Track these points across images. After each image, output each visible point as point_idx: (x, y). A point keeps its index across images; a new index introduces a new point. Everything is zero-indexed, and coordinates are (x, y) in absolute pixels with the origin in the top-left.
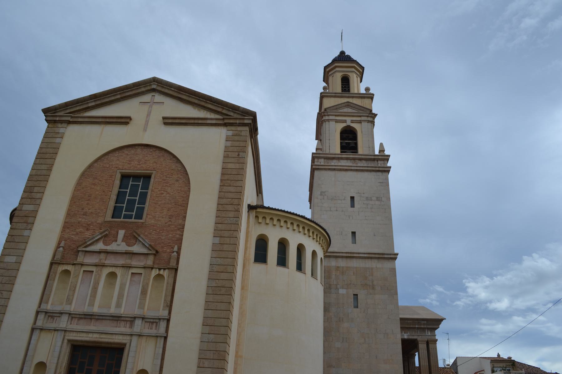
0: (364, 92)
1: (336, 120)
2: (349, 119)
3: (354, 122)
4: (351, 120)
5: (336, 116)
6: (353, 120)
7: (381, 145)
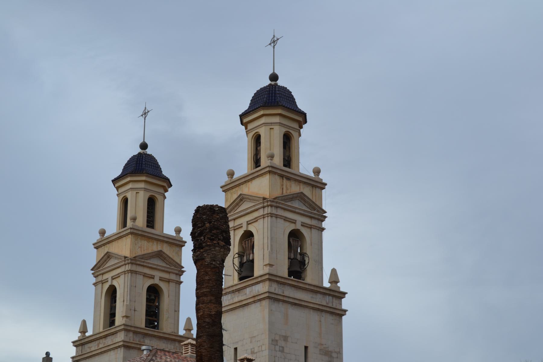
0: (312, 175)
1: (286, 217)
2: (300, 219)
3: (304, 225)
4: (302, 222)
5: (285, 209)
6: (304, 223)
7: (334, 272)
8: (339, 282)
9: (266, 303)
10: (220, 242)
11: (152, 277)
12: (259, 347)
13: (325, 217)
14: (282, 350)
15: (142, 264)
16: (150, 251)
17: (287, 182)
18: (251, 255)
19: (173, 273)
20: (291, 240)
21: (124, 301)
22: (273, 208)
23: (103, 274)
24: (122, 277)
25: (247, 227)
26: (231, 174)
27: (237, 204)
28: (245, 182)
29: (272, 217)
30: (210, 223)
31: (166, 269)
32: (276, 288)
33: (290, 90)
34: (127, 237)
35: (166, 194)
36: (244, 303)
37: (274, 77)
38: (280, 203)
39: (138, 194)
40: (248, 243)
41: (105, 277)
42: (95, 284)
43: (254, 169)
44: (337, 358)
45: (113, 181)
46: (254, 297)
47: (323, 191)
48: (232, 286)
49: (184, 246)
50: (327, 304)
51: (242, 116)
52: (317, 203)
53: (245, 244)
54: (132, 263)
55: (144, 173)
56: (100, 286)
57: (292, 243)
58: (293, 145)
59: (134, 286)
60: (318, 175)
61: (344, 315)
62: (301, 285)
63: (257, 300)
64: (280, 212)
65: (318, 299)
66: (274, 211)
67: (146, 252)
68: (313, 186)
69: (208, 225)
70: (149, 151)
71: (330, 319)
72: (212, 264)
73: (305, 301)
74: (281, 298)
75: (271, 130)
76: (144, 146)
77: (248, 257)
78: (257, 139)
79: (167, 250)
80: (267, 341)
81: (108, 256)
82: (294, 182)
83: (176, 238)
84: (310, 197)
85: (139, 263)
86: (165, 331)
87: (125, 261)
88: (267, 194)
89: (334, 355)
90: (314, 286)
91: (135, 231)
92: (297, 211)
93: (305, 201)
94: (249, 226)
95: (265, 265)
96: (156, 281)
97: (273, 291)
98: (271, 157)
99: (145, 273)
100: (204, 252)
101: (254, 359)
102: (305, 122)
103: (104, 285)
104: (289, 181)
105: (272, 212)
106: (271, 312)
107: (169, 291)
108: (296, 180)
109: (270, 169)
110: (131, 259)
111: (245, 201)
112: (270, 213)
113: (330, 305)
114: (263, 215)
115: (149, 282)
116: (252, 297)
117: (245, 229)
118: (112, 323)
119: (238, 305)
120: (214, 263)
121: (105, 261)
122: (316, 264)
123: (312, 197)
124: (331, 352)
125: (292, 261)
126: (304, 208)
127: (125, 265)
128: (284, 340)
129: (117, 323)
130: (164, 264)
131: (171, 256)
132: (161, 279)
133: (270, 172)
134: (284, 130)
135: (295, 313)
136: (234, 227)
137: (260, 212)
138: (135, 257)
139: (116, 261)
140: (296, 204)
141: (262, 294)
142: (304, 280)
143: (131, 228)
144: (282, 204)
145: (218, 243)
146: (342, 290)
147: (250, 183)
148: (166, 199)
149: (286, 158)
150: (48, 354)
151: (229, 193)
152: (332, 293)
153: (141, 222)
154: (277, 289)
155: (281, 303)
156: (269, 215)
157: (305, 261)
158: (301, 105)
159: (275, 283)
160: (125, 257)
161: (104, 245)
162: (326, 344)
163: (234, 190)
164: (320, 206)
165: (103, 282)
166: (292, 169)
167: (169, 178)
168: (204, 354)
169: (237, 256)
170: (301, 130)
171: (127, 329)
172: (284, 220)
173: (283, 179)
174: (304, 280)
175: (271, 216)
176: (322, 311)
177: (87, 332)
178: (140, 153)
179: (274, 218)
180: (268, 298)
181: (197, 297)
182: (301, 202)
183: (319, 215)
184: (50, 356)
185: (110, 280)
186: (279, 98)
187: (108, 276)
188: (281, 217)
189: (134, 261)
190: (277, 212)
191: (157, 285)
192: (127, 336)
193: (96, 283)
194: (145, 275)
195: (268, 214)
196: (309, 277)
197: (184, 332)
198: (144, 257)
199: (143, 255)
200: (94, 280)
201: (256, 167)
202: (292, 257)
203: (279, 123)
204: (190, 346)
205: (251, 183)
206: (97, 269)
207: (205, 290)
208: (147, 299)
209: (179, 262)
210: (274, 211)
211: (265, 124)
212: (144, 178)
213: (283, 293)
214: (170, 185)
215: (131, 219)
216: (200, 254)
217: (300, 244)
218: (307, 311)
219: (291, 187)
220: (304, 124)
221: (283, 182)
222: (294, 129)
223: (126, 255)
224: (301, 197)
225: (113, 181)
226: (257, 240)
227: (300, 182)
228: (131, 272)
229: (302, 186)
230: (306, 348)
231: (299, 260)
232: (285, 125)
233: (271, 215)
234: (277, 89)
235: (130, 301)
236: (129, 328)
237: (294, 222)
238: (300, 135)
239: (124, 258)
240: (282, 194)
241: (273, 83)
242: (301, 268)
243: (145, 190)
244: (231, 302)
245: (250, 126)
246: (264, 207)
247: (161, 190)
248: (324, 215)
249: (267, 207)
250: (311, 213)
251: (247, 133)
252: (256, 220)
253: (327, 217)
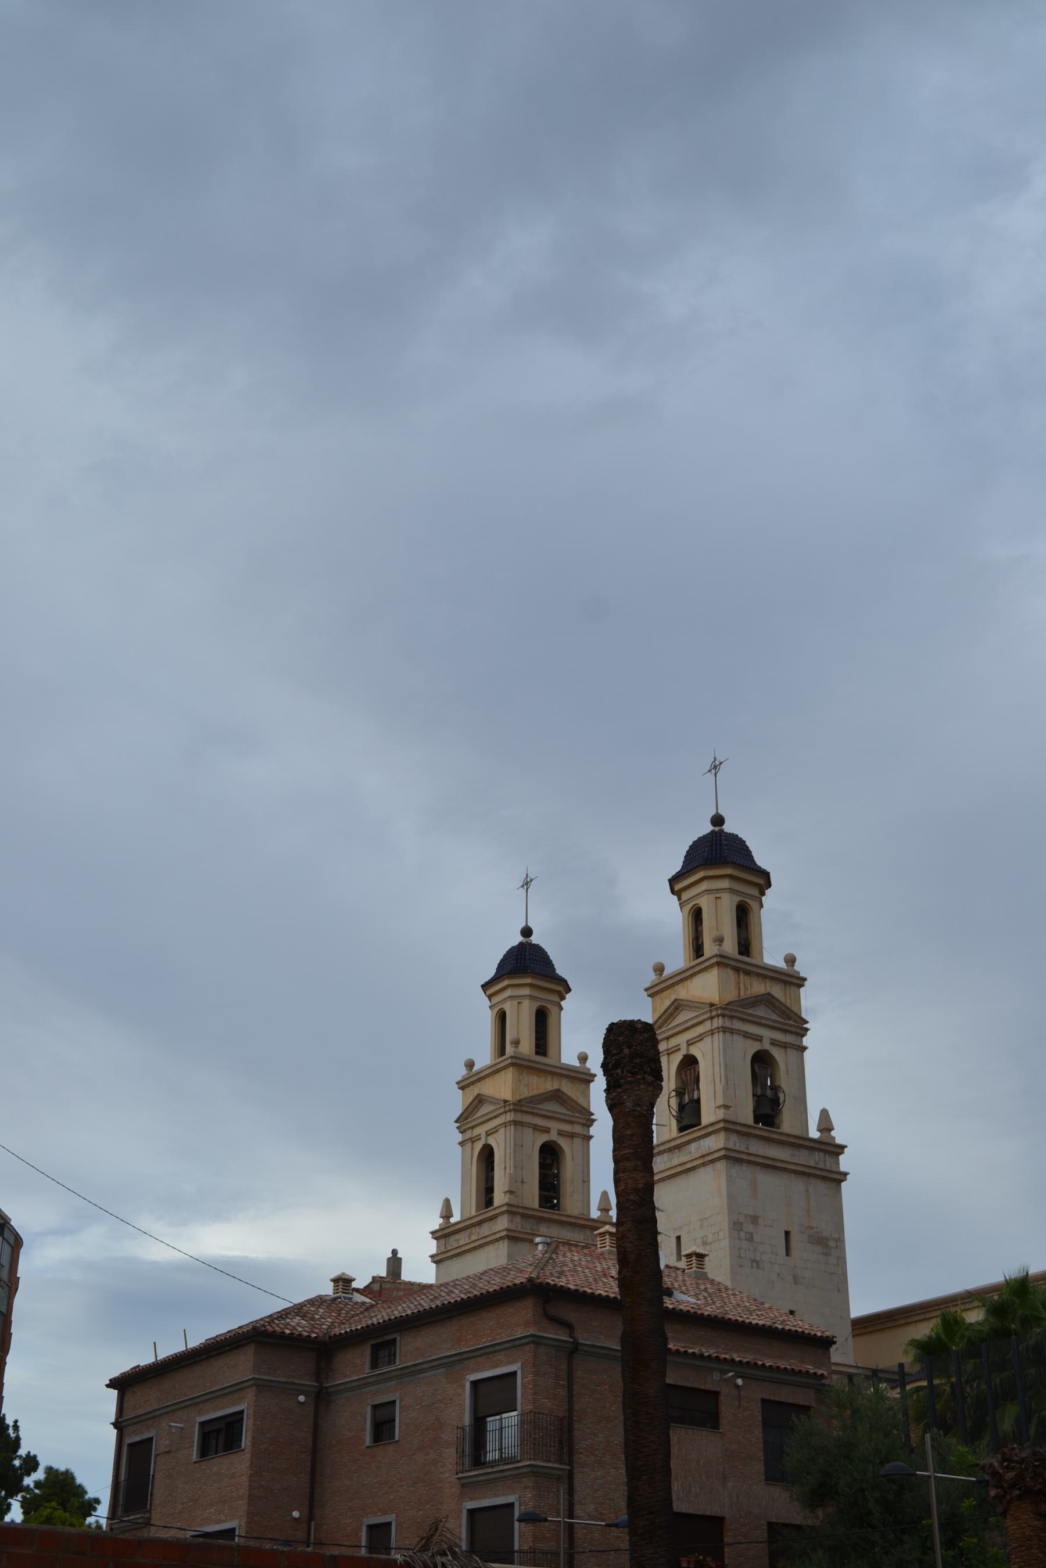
2: (767, 1034)
4: (771, 1039)
5: (743, 1020)
6: (774, 1040)
7: (824, 1114)
8: (833, 1129)
9: (721, 1166)
10: (646, 1076)
11: (547, 1131)
12: (714, 1234)
13: (807, 1030)
14: (750, 1238)
15: (531, 1110)
16: (542, 1091)
17: (746, 978)
18: (696, 1092)
19: (579, 1123)
20: (756, 1068)
21: (505, 1168)
22: (726, 1018)
23: (472, 1128)
24: (502, 1131)
25: (688, 1049)
26: (659, 969)
27: (671, 1015)
28: (682, 980)
29: (724, 1032)
30: (630, 1047)
31: (567, 1118)
32: (735, 1143)
33: (744, 839)
34: (507, 1070)
35: (563, 1003)
36: (689, 1166)
37: (718, 820)
38: (736, 1011)
39: (520, 1005)
40: (690, 1075)
41: (477, 1131)
42: (461, 1144)
43: (693, 960)
44: (837, 1247)
45: (483, 986)
46: (703, 1156)
47: (802, 989)
48: (669, 1141)
49: (593, 1081)
50: (817, 1164)
51: (672, 881)
52: (793, 1009)
53: (686, 1076)
54: (515, 1110)
55: (528, 973)
56: (469, 1145)
57: (757, 1071)
58: (752, 921)
59: (520, 1144)
60: (793, 966)
61: (843, 1181)
62: (775, 1136)
63: (708, 1161)
64: (737, 1025)
65: (802, 1158)
66: (728, 1024)
67: (536, 1092)
68: (786, 983)
69: (626, 1051)
70: (534, 939)
71: (822, 1187)
72: (635, 1110)
74: (745, 1157)
75: (718, 900)
76: (527, 932)
77: (691, 1095)
78: (697, 915)
79: (568, 1088)
80: (726, 1225)
81: (480, 1100)
83: (581, 1070)
84: (783, 1000)
85: (525, 1109)
86: (569, 1212)
87: (505, 1107)
88: (715, 998)
89: (832, 1244)
90: (795, 1137)
91: (519, 1062)
92: (763, 1021)
94: (691, 1047)
95: (719, 1107)
96: (553, 1136)
97: (731, 1145)
98: (720, 940)
99: (536, 1125)
100: (622, 1092)
101: (707, 1253)
102: (769, 885)
103: (475, 1144)
104: (748, 977)
105: (725, 1026)
106: (730, 1179)
107: (572, 1151)
108: (759, 975)
109: (719, 959)
110: (514, 1104)
111: (682, 1010)
112: (722, 1027)
113: (821, 1166)
114: (712, 1030)
115: (543, 1138)
116: (699, 1158)
117: (685, 1053)
118: (489, 1202)
119: (679, 1169)
120: (638, 1109)
121: (476, 1107)
123: (786, 1002)
124: (827, 1239)
125: (759, 1100)
126: (774, 1017)
127: (506, 1112)
128: (753, 1223)
129: (497, 1202)
130: (564, 1111)
131: (574, 1098)
132: (561, 1133)
133: (718, 964)
134: (737, 899)
135: (767, 1181)
136: (668, 1050)
137: (707, 1026)
138: (519, 1101)
139: (492, 1108)
140: (761, 1011)
141: (715, 1152)
142: (779, 1128)
143: (512, 1057)
144: (740, 1012)
145: (644, 1079)
146: (838, 1141)
147: (689, 982)
148: (562, 1011)
149: (743, 942)
150: (394, 1252)
151: (657, 998)
152: (822, 1147)
153: (527, 1047)
154: (738, 1144)
155: (745, 1165)
156: (721, 1029)
157: (779, 1098)
158: (761, 860)
159: (735, 1134)
160: (505, 1101)
161: (473, 1083)
162: (817, 1228)
163: (665, 993)
164: (798, 1013)
165: (473, 1140)
166: (752, 958)
167: (566, 979)
168: (629, 1250)
169: (674, 1094)
170: (763, 898)
171: (512, 1210)
172: (744, 1036)
173: (739, 974)
174: (779, 1128)
175: (723, 1031)
176: (809, 1175)
177: (452, 1216)
178: (521, 944)
179: (728, 1035)
180: (725, 1157)
181: (614, 1161)
183: (797, 1027)
184: (398, 1256)
185: (483, 1136)
186: (726, 851)
187: (481, 1130)
188: (739, 1032)
189: (519, 1106)
190: (732, 1024)
191: (554, 1142)
192: (512, 1221)
193: (463, 1142)
194: (536, 1128)
195: (718, 1028)
196: (787, 1124)
197: (599, 1213)
198: (534, 1100)
199: (533, 1097)
200: (459, 1137)
201: (698, 957)
202: (759, 1092)
203: (730, 889)
204: (607, 1236)
205: (691, 981)
206: (464, 1121)
207: (626, 1151)
208: (540, 1164)
209: (586, 1107)
210: (728, 1024)
211: (708, 891)
212: (528, 981)
213: (748, 1149)
214: (568, 990)
215: (512, 1043)
216: (616, 1096)
217: (769, 1072)
219: (751, 985)
220: (767, 889)
221: (739, 978)
222: (752, 897)
223: (507, 1099)
224: (767, 1000)
225: (483, 986)
226: (704, 1068)
227: (765, 977)
228: (516, 1123)
229: (768, 983)
230: (787, 1234)
231: (770, 1096)
232: (737, 891)
233: (724, 1030)
234: (723, 838)
235: (515, 1167)
236: (515, 1210)
237: (759, 1039)
238: (761, 906)
239: (502, 1102)
240: (739, 996)
241: (717, 829)
242: (773, 1111)
243: (532, 998)
244: (669, 1166)
245: (685, 896)
246: (712, 1018)
247: (556, 998)
248: (805, 1026)
249: (717, 1018)
250: (785, 1024)
251: (681, 905)
252: (701, 1038)
253: (809, 1029)
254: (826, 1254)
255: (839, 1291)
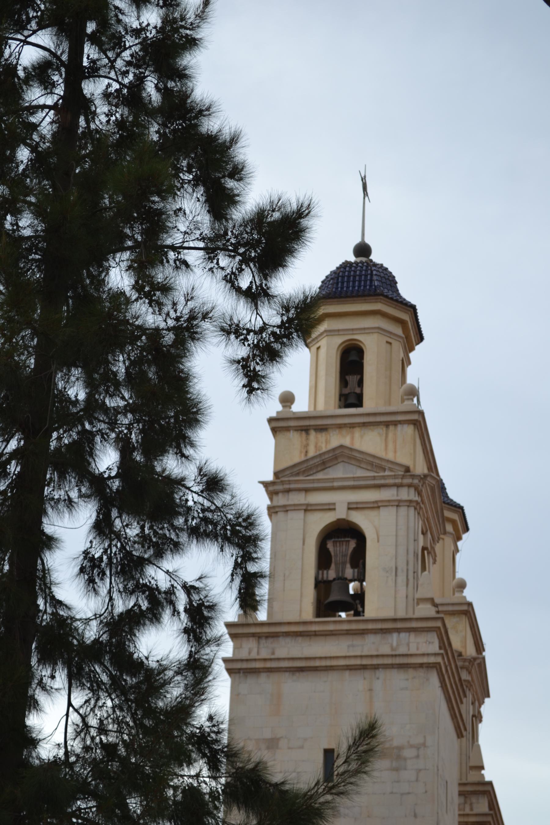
20: (330, 546)
38: (290, 482)
44: (418, 757)
62: (331, 627)
73: (321, 658)
82: (337, 431)
92: (336, 484)
93: (355, 459)
122: (387, 577)
124: (400, 748)
134: (339, 340)
172: (306, 510)
176: (376, 667)
182: (351, 464)
218: (333, 676)
254: (397, 769)
255: (415, 816)
